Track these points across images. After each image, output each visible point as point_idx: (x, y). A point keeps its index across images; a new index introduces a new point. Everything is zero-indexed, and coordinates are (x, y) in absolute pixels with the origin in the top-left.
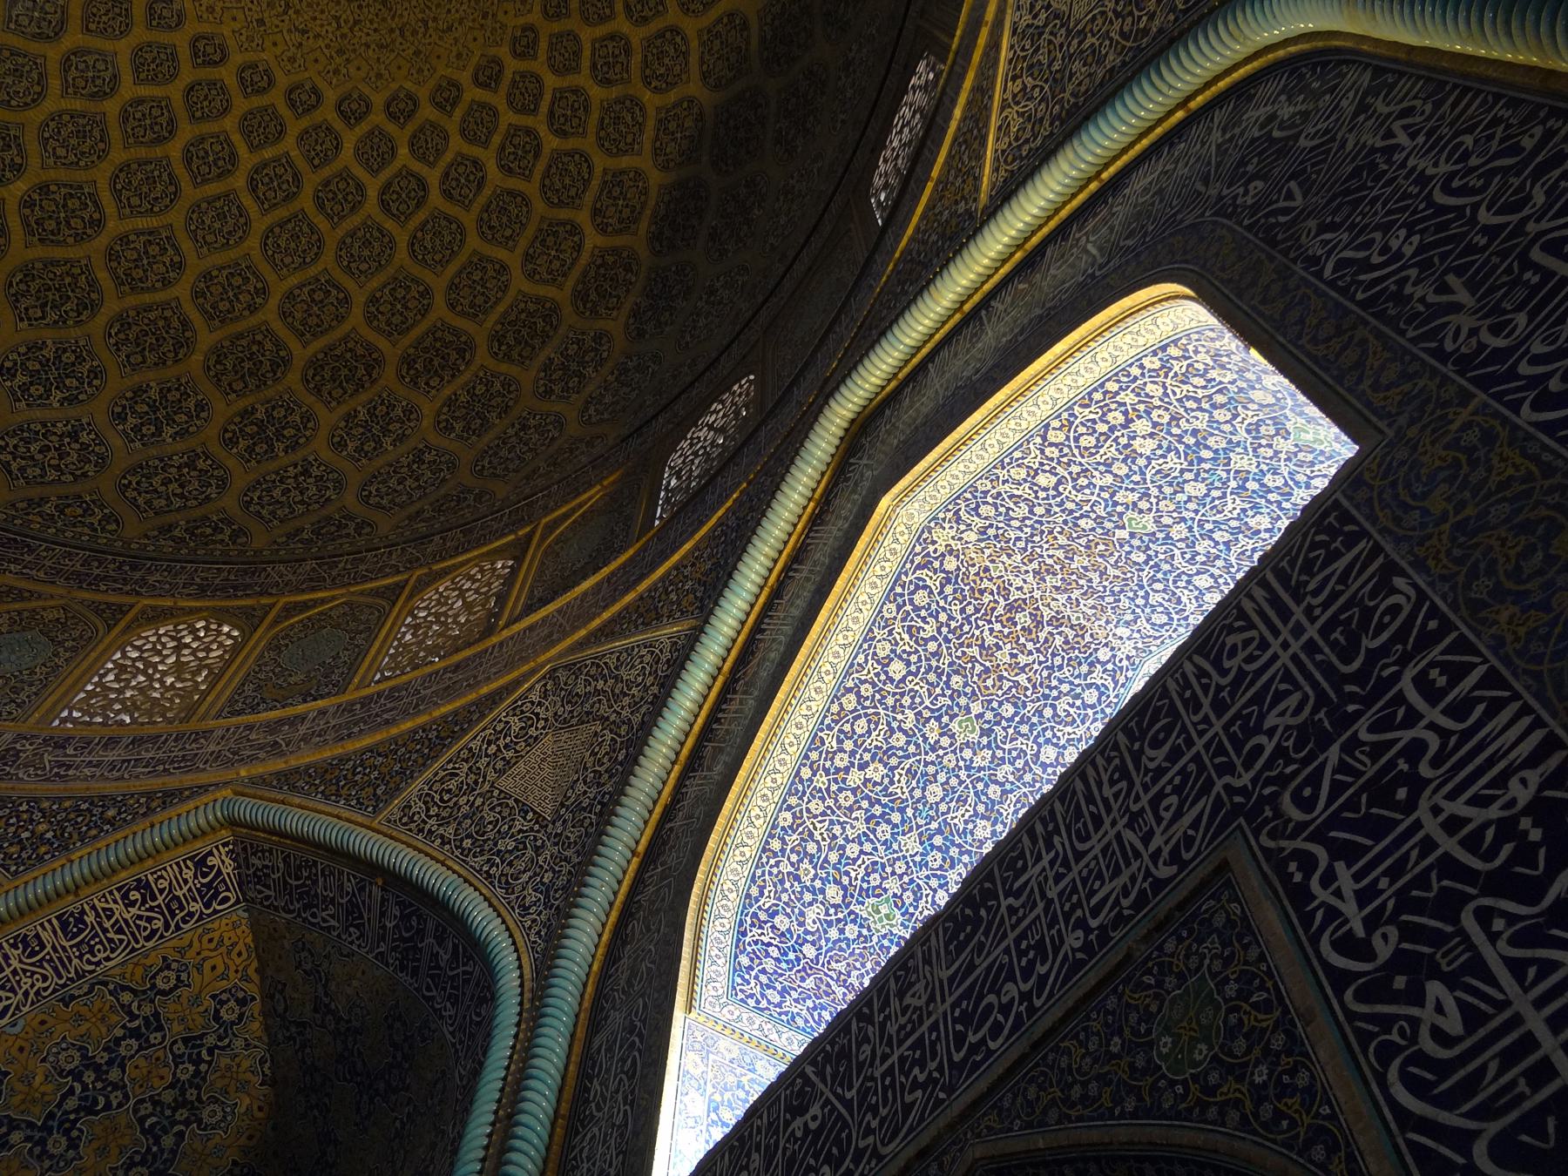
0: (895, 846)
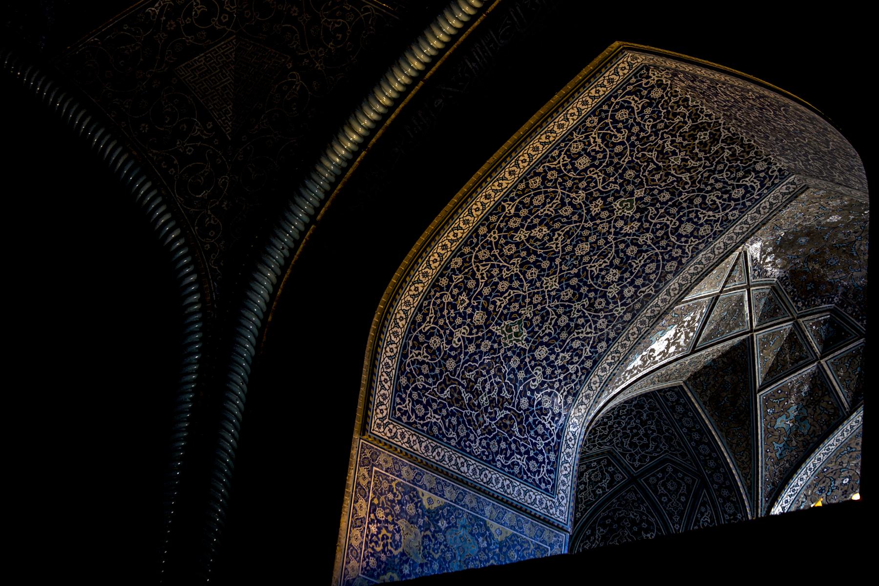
0: (538, 284)
